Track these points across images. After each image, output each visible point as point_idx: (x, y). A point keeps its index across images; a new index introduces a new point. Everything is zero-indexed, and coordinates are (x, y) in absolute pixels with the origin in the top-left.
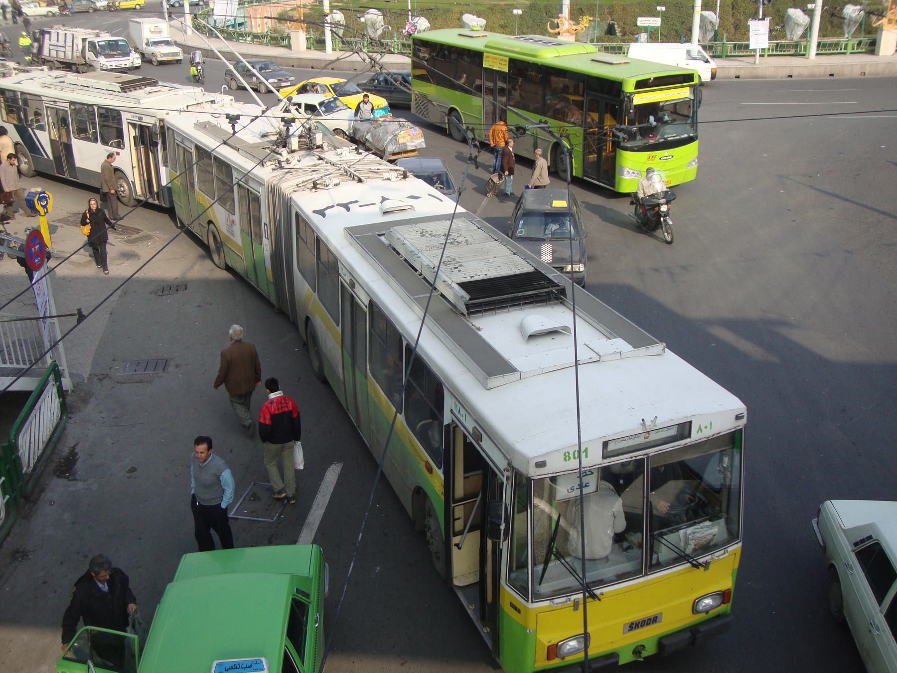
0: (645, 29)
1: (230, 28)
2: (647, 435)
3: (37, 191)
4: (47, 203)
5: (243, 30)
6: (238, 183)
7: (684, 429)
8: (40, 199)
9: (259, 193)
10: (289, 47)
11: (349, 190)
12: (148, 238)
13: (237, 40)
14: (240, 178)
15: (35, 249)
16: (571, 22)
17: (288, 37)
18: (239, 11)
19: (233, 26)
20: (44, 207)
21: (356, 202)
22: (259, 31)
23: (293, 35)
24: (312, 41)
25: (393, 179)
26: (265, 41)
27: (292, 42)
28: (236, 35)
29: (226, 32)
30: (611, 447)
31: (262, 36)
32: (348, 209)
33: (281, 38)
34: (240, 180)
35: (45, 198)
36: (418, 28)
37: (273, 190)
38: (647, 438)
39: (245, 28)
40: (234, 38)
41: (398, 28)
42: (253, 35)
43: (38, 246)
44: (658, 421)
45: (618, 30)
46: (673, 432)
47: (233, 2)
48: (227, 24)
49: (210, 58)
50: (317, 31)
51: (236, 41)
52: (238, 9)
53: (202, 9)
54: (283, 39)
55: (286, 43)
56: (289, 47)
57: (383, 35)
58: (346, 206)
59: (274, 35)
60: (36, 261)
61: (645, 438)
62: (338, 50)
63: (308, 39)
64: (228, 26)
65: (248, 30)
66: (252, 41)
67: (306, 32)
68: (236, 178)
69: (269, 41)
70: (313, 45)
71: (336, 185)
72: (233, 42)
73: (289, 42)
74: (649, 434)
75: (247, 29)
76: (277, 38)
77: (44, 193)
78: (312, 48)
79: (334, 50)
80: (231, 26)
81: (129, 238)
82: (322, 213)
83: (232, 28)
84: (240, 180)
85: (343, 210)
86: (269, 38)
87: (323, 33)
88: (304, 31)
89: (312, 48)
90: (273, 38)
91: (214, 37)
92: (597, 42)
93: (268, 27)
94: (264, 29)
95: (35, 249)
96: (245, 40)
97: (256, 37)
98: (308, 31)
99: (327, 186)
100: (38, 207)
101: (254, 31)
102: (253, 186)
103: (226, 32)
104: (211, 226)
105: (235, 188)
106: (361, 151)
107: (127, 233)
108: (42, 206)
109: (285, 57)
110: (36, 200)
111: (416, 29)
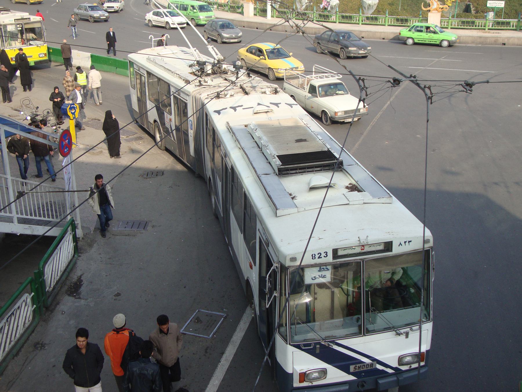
0: (493, 9)
2: (363, 248)
3: (69, 103)
4: (75, 111)
6: (173, 94)
7: (388, 246)
8: (71, 108)
9: (187, 101)
10: (242, 13)
11: (240, 98)
14: (175, 92)
15: (65, 142)
16: (439, 3)
17: (242, 6)
20: (73, 114)
21: (242, 106)
23: (245, 5)
24: (258, 10)
25: (268, 92)
26: (226, 8)
27: (244, 10)
30: (340, 253)
31: (224, 5)
32: (235, 110)
34: (175, 93)
35: (74, 108)
36: (331, 4)
37: (196, 100)
38: (363, 249)
41: (317, 3)
43: (67, 141)
44: (369, 238)
45: (472, 9)
46: (381, 247)
50: (261, 3)
54: (238, 8)
55: (240, 10)
56: (242, 13)
57: (306, 9)
58: (234, 108)
59: (232, 5)
60: (66, 150)
61: (362, 250)
62: (275, 17)
63: (255, 9)
66: (218, 8)
67: (254, 4)
68: (173, 92)
69: (229, 9)
70: (259, 12)
71: (231, 96)
73: (242, 10)
74: (364, 247)
76: (235, 7)
77: (74, 104)
78: (258, 15)
79: (272, 17)
81: (127, 138)
82: (218, 112)
84: (175, 93)
85: (232, 110)
86: (229, 7)
87: (266, 5)
88: (252, 3)
89: (258, 15)
90: (231, 7)
92: (456, 18)
95: (65, 142)
98: (255, 3)
99: (226, 96)
100: (69, 114)
102: (183, 96)
104: (156, 123)
105: (172, 97)
106: (251, 75)
108: (72, 113)
109: (238, 20)
111: (329, 4)
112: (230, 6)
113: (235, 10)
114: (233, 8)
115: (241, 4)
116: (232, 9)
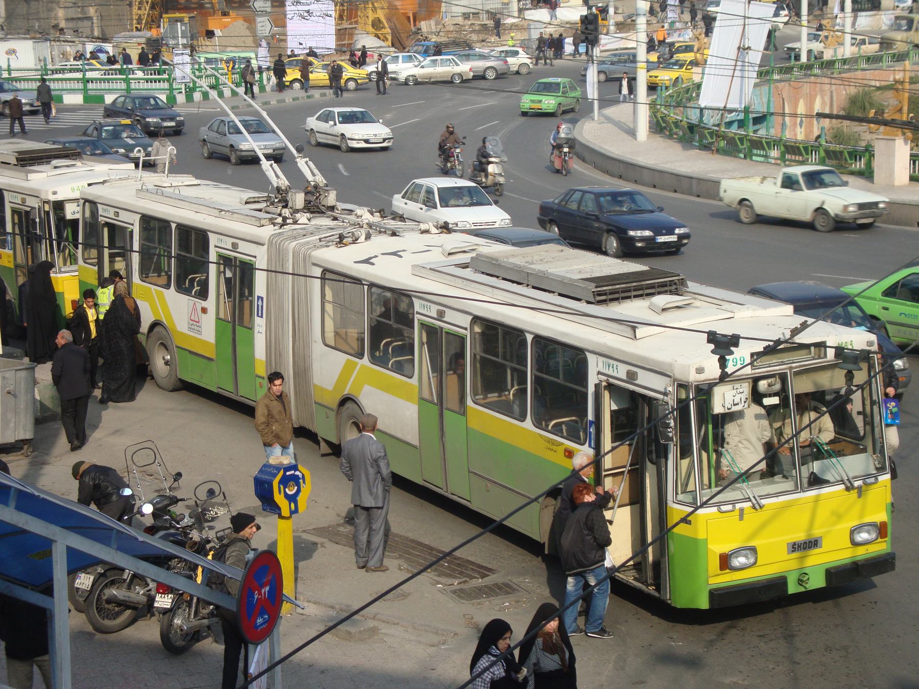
1: (734, 129)
3: (281, 464)
4: (298, 491)
5: (762, 132)
8: (285, 481)
10: (867, 174)
12: (505, 589)
15: (260, 594)
17: (869, 151)
18: (758, 89)
19: (741, 124)
20: (292, 499)
23: (879, 148)
27: (877, 164)
28: (746, 144)
29: (724, 138)
31: (806, 149)
33: (849, 153)
35: (295, 479)
39: (767, 130)
40: (740, 151)
43: (267, 589)
48: (730, 117)
49: (683, 193)
51: (745, 157)
54: (855, 155)
55: (860, 165)
56: (867, 174)
60: (259, 621)
64: (729, 124)
66: (782, 158)
72: (737, 160)
73: (869, 165)
75: (772, 132)
76: (841, 153)
77: (295, 468)
80: (736, 125)
81: (463, 586)
83: (739, 127)
86: (823, 154)
88: (906, 140)
93: (823, 129)
94: (812, 131)
95: (260, 594)
96: (766, 156)
100: (279, 499)
101: (788, 135)
103: (724, 138)
107: (461, 573)
108: (287, 496)
110: (275, 484)
112: (827, 152)
113: (843, 163)
114: (837, 158)
115: (863, 144)
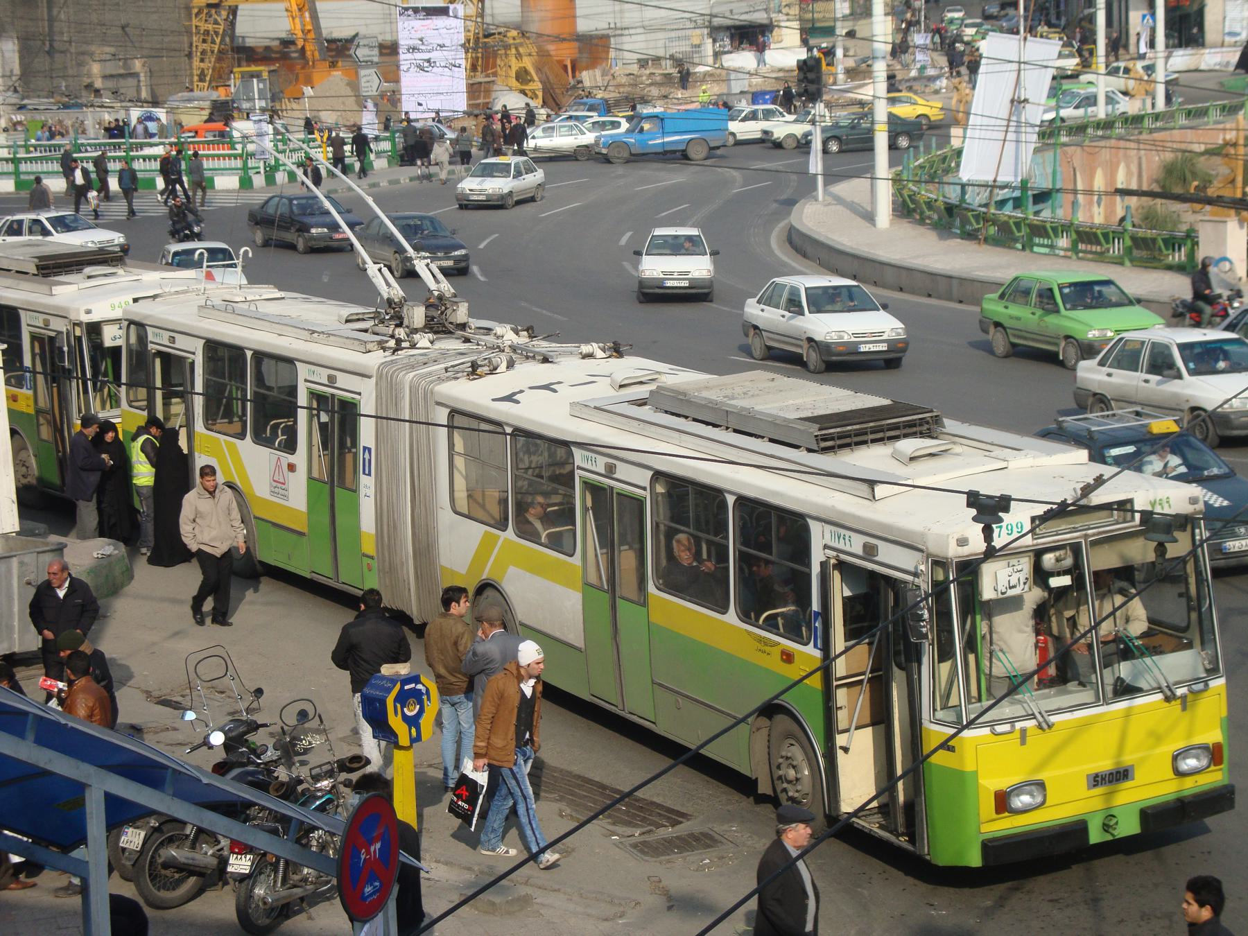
1: (1008, 210)
3: (397, 674)
5: (1046, 214)
8: (402, 699)
12: (704, 841)
13: (1028, 246)
15: (368, 852)
17: (1191, 237)
18: (1039, 155)
19: (1018, 203)
20: (413, 722)
22: (1099, 219)
23: (1205, 234)
26: (1116, 249)
28: (1025, 231)
31: (1105, 235)
33: (1165, 241)
35: (417, 695)
40: (1016, 240)
42: (1078, 233)
43: (378, 845)
47: (1023, 137)
48: (1001, 194)
49: (939, 298)
51: (1024, 248)
52: (1036, 151)
53: (928, 149)
54: (1173, 243)
59: (1141, 233)
60: (368, 889)
64: (1002, 203)
65: (1062, 214)
66: (1074, 248)
69: (1128, 251)
72: (1012, 252)
75: (1060, 213)
76: (1154, 240)
77: (416, 679)
80: (1010, 204)
81: (647, 838)
86: (1128, 242)
90: (1138, 242)
91: (955, 236)
93: (1128, 208)
95: (368, 852)
96: (1052, 247)
97: (1086, 237)
100: (395, 722)
101: (1081, 217)
103: (994, 222)
107: (643, 819)
108: (405, 718)
113: (1156, 254)
114: (1147, 247)
115: (1184, 228)
116: (1144, 254)
